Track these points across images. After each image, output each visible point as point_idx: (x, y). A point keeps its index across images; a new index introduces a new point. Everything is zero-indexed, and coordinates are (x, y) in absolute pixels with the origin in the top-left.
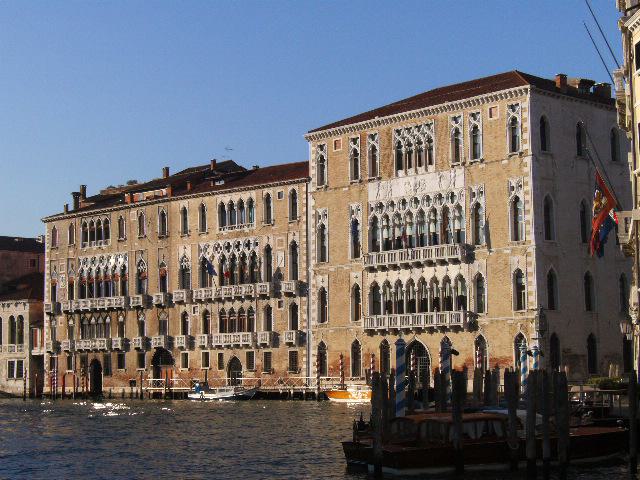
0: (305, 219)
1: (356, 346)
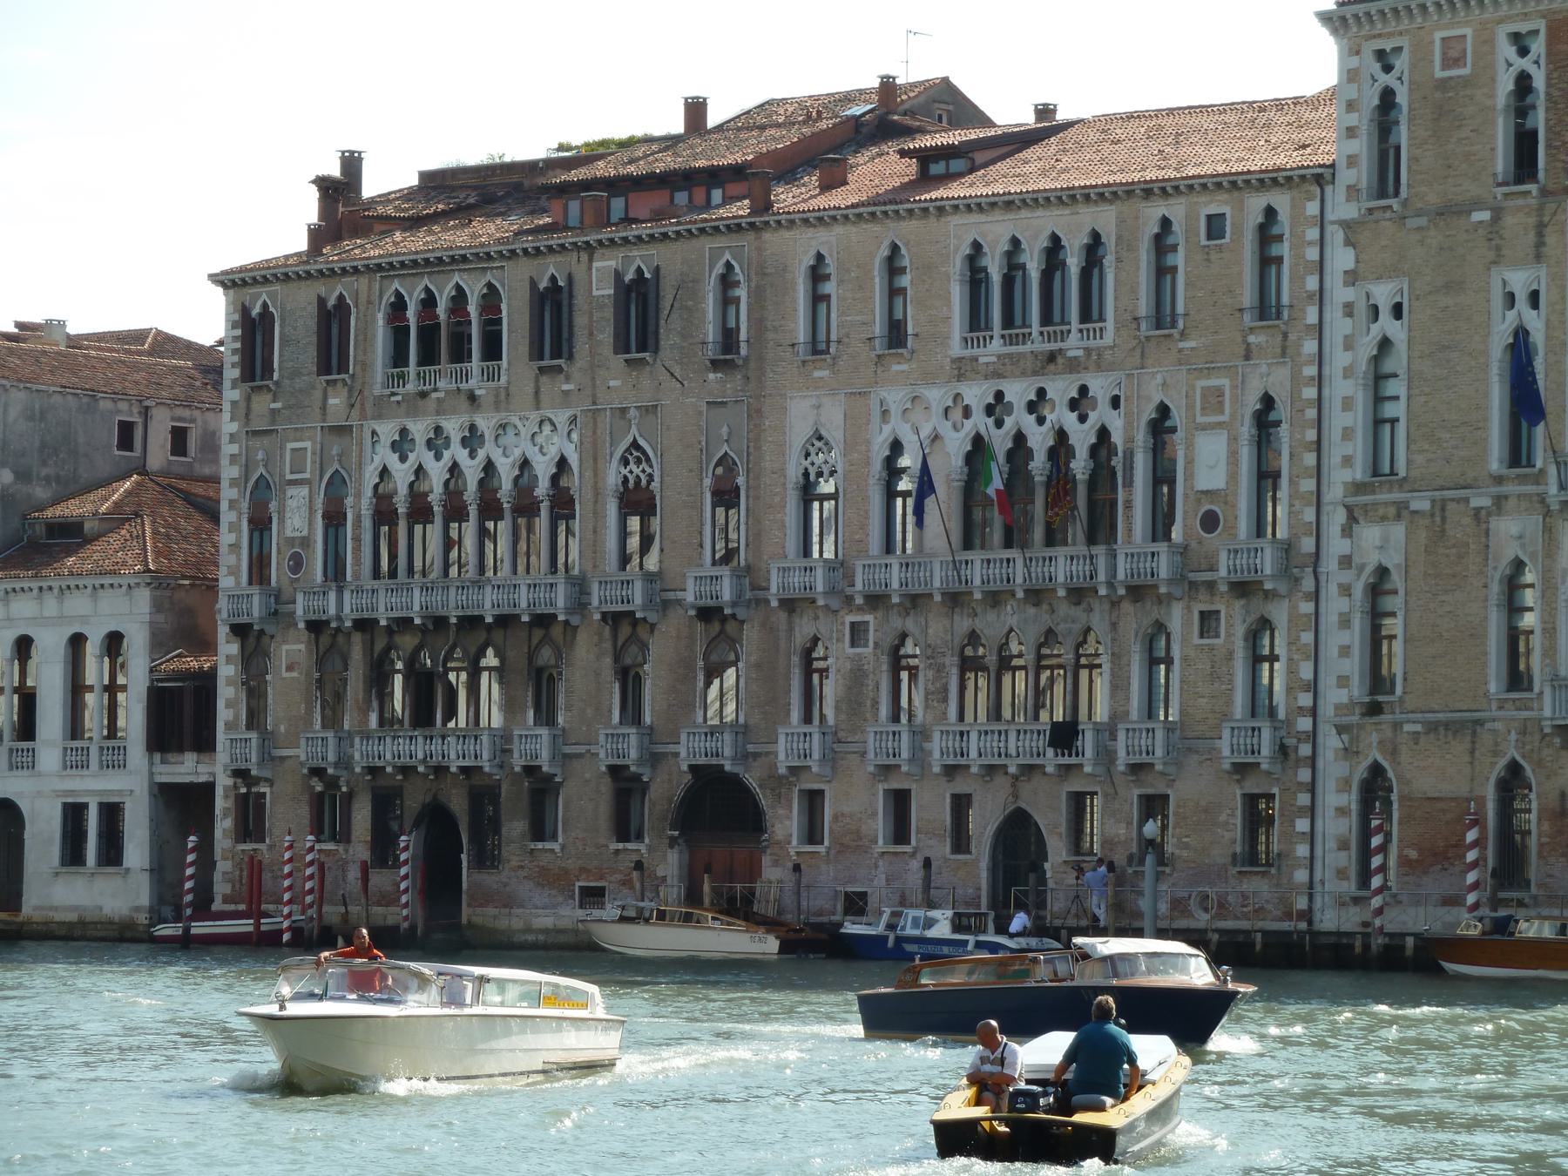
1: (1512, 781)
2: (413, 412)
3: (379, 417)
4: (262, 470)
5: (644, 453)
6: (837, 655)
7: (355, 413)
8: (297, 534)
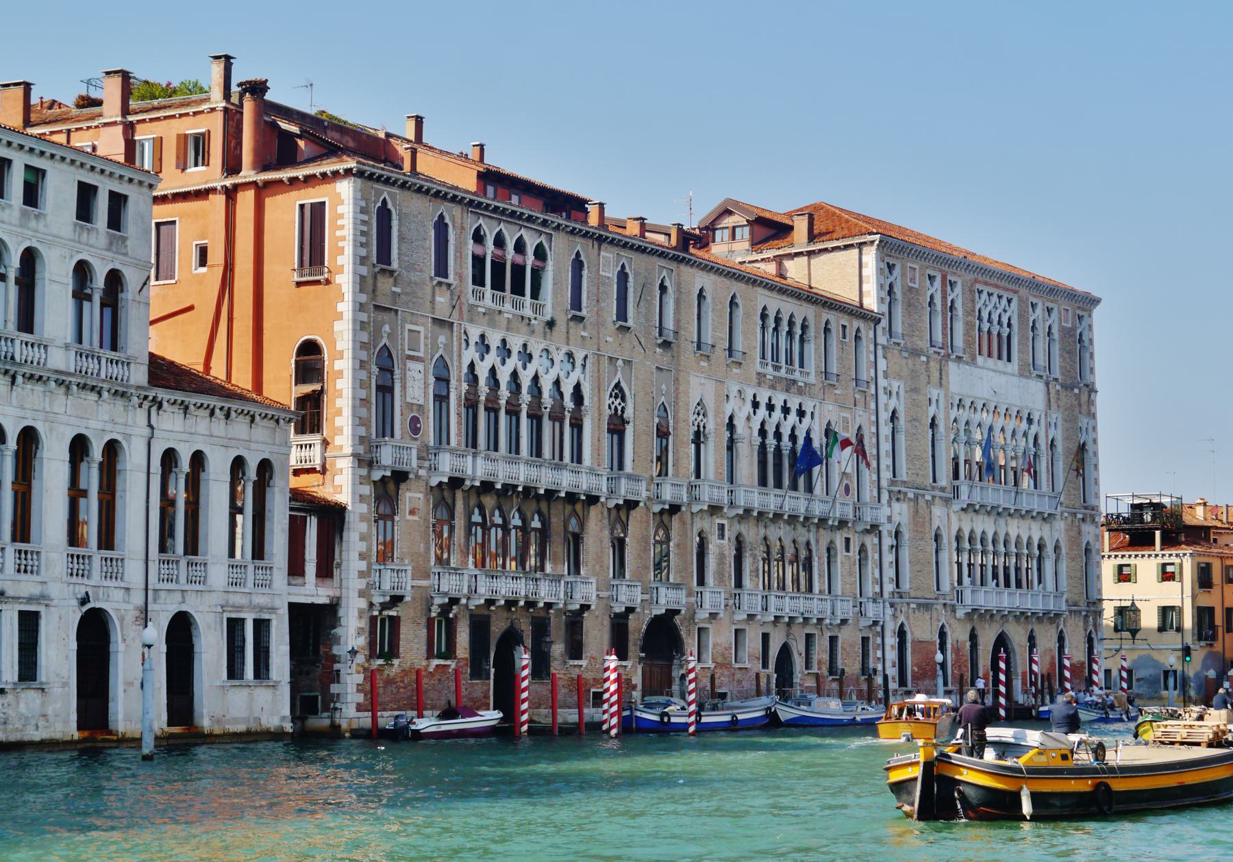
0: (873, 391)
2: (493, 324)
3: (471, 321)
4: (384, 341)
5: (622, 391)
7: (456, 313)
8: (415, 401)
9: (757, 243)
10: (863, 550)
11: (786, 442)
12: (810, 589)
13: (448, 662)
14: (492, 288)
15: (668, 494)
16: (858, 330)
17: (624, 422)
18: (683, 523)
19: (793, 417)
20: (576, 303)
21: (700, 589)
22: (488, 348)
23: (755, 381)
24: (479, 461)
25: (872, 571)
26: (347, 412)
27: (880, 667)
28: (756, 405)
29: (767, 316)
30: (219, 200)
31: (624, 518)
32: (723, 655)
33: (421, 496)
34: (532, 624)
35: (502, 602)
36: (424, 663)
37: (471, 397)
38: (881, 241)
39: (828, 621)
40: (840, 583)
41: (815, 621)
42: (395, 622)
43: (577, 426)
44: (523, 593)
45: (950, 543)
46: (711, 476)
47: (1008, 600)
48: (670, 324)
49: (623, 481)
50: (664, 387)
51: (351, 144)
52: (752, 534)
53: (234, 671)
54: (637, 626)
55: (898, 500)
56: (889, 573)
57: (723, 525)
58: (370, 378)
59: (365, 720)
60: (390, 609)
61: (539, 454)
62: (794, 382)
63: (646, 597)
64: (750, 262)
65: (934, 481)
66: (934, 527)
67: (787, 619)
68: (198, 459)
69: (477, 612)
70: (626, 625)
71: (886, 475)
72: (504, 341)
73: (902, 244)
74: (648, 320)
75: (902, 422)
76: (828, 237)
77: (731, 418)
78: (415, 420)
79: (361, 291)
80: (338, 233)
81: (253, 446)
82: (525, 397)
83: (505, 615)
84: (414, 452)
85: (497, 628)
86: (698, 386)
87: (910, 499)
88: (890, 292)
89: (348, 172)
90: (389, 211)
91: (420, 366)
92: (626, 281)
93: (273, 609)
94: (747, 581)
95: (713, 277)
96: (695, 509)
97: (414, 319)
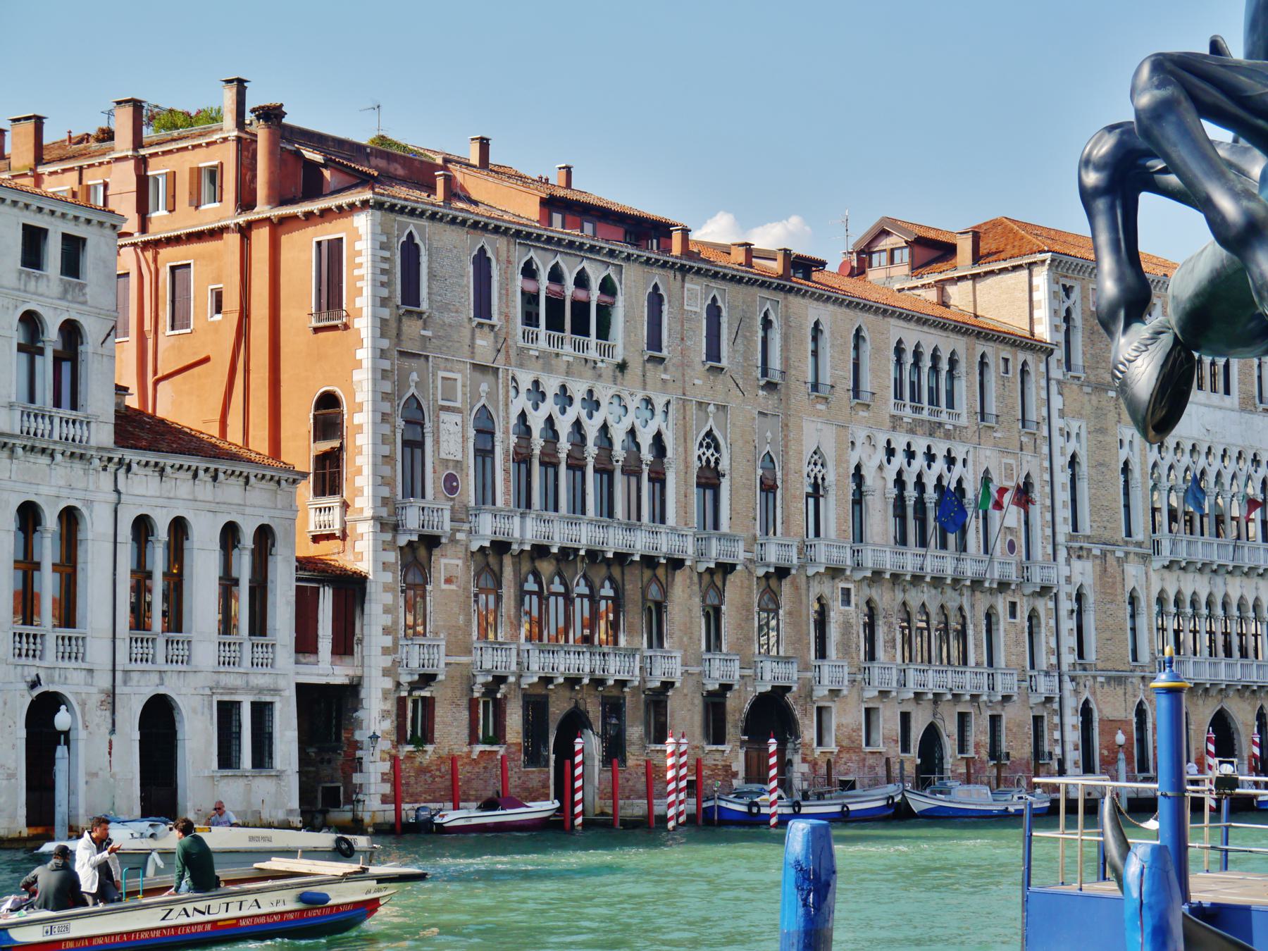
0: (1046, 433)
2: (548, 369)
3: (521, 366)
4: (412, 390)
5: (714, 439)
6: (836, 613)
7: (501, 357)
8: (451, 457)
9: (917, 267)
10: (1033, 616)
11: (931, 495)
12: (964, 661)
13: (495, 748)
14: (547, 328)
15: (773, 555)
16: (1025, 364)
17: (719, 475)
18: (797, 588)
19: (940, 465)
20: (655, 341)
21: (819, 662)
22: (543, 395)
23: (888, 423)
24: (529, 522)
25: (1045, 640)
26: (367, 470)
27: (1058, 750)
28: (890, 452)
29: (903, 350)
30: (233, 239)
31: (719, 584)
32: (850, 738)
33: (460, 562)
34: (603, 704)
35: (561, 680)
36: (466, 749)
37: (523, 451)
38: (1053, 260)
39: (985, 698)
40: (1003, 653)
41: (968, 698)
42: (429, 703)
43: (658, 479)
44: (587, 670)
45: (1149, 606)
46: (833, 534)
47: (1226, 671)
48: (775, 362)
49: (714, 542)
50: (769, 434)
51: (400, 172)
52: (887, 599)
53: (227, 758)
54: (737, 706)
55: (1079, 557)
56: (1070, 641)
57: (849, 590)
58: (394, 432)
59: (389, 813)
60: (421, 689)
61: (611, 514)
62: (940, 424)
63: (747, 672)
64: (909, 289)
65: (1129, 534)
66: (1128, 588)
67: (930, 696)
68: (179, 527)
69: (531, 691)
70: (723, 705)
71: (1064, 529)
72: (563, 388)
73: (1081, 262)
74: (746, 359)
75: (1084, 469)
76: (995, 257)
77: (858, 468)
78: (450, 479)
79: (383, 336)
80: (356, 272)
81: (248, 510)
82: (591, 450)
83: (567, 694)
84: (447, 515)
85: (558, 708)
86: (814, 432)
87: (1096, 557)
88: (1068, 318)
89: (365, 204)
90: (417, 246)
91: (457, 418)
92: (719, 316)
93: (276, 691)
94: (880, 653)
95: (831, 307)
96: (811, 572)
97: (449, 365)
